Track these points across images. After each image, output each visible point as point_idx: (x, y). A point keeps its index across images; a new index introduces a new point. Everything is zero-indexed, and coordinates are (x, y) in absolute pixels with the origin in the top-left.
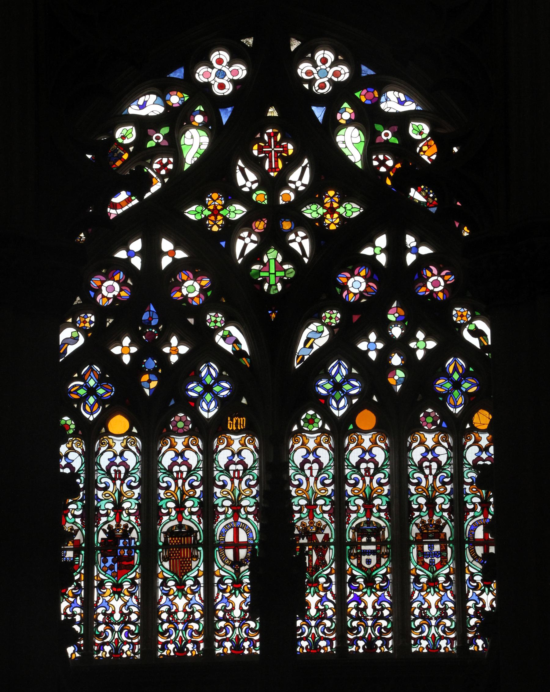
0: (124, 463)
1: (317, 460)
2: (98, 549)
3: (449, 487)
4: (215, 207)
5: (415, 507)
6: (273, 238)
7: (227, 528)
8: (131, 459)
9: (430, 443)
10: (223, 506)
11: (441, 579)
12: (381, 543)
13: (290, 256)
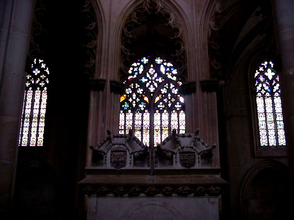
13: (154, 87)
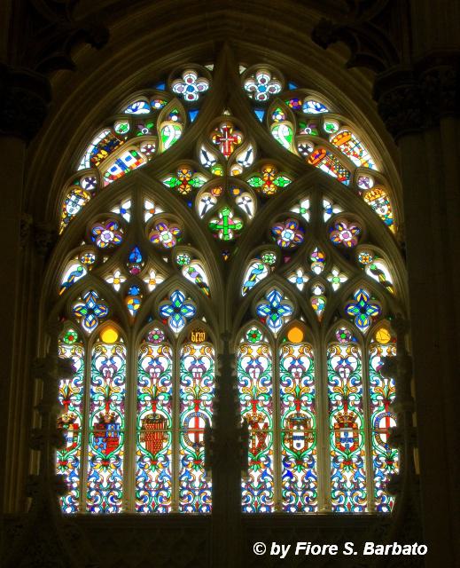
0: (113, 365)
1: (258, 365)
3: (359, 388)
4: (185, 180)
5: (334, 402)
6: (227, 200)
7: (190, 416)
8: (119, 363)
9: (344, 354)
11: (354, 459)
13: (239, 213)
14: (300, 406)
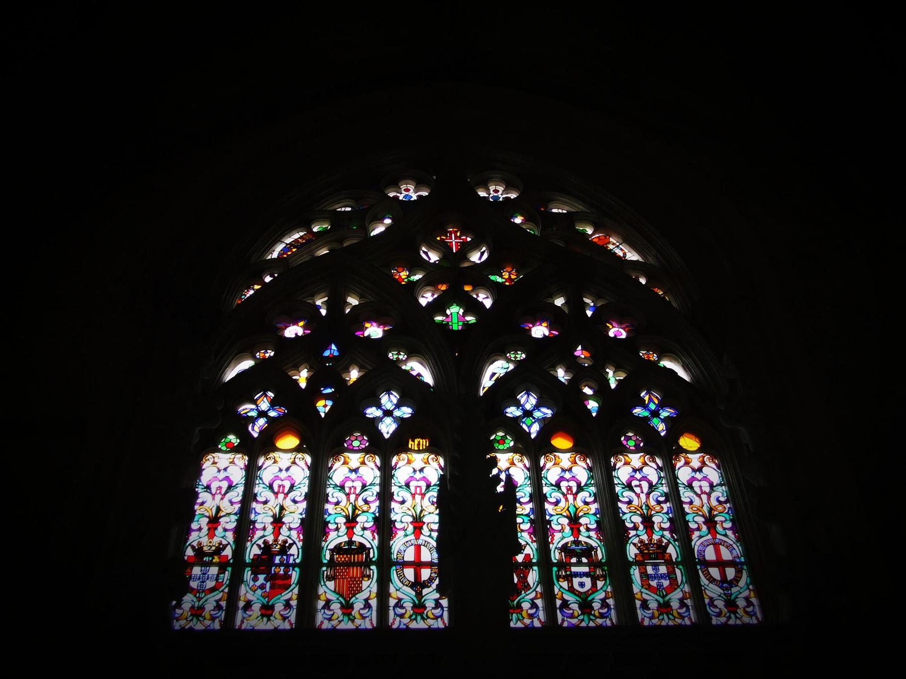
2: (248, 565)
5: (630, 525)
10: (401, 522)
11: (675, 605)
12: (594, 564)
14: (579, 531)
